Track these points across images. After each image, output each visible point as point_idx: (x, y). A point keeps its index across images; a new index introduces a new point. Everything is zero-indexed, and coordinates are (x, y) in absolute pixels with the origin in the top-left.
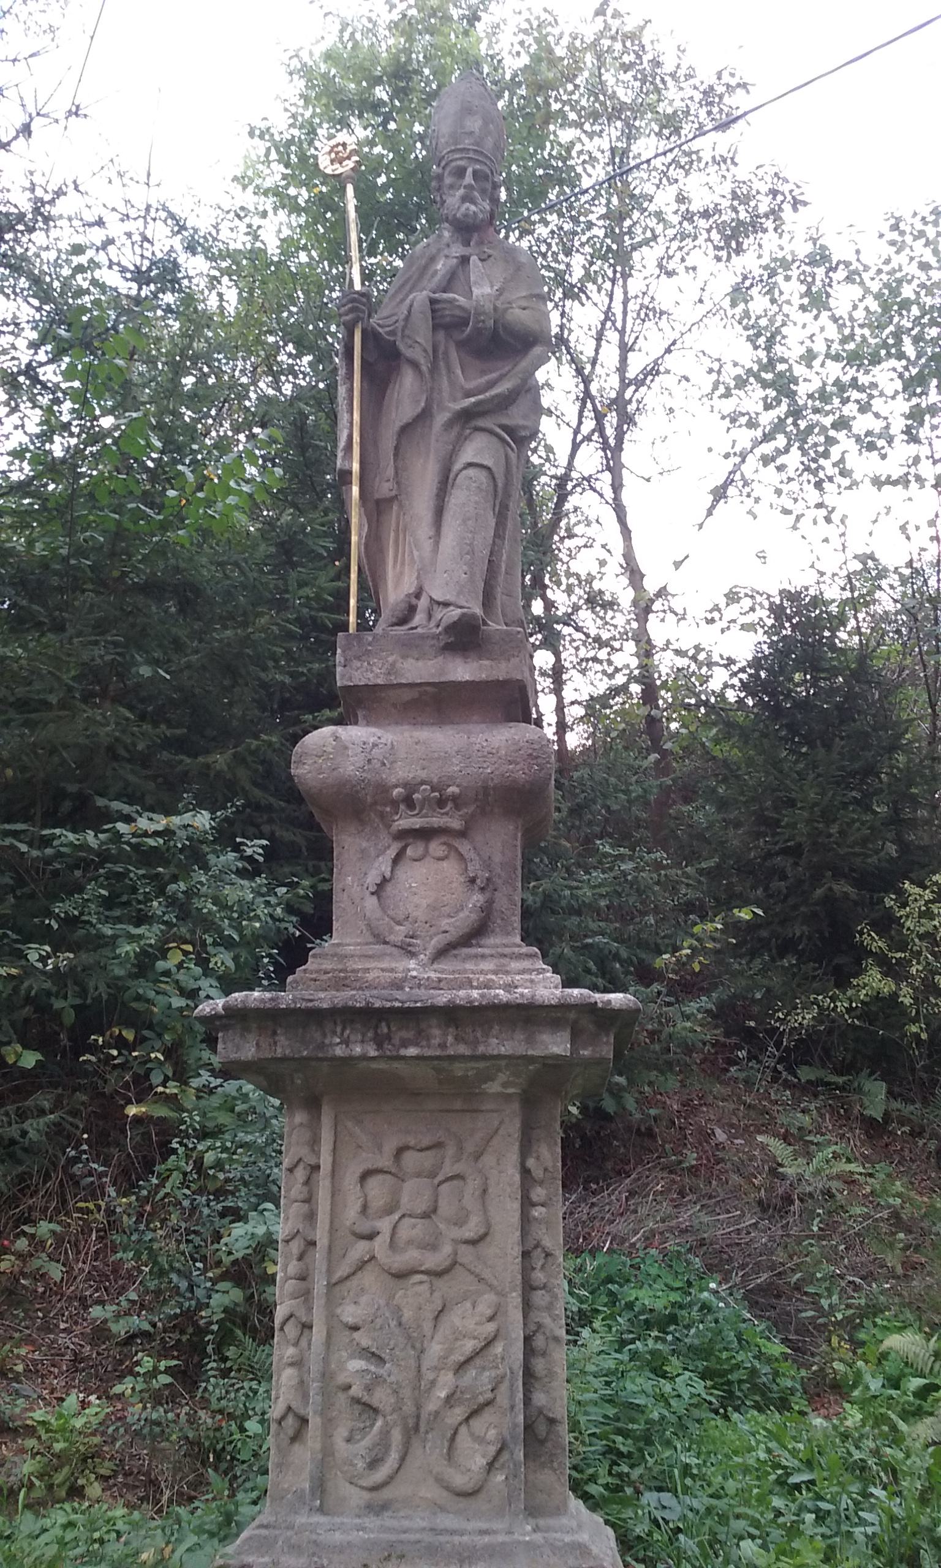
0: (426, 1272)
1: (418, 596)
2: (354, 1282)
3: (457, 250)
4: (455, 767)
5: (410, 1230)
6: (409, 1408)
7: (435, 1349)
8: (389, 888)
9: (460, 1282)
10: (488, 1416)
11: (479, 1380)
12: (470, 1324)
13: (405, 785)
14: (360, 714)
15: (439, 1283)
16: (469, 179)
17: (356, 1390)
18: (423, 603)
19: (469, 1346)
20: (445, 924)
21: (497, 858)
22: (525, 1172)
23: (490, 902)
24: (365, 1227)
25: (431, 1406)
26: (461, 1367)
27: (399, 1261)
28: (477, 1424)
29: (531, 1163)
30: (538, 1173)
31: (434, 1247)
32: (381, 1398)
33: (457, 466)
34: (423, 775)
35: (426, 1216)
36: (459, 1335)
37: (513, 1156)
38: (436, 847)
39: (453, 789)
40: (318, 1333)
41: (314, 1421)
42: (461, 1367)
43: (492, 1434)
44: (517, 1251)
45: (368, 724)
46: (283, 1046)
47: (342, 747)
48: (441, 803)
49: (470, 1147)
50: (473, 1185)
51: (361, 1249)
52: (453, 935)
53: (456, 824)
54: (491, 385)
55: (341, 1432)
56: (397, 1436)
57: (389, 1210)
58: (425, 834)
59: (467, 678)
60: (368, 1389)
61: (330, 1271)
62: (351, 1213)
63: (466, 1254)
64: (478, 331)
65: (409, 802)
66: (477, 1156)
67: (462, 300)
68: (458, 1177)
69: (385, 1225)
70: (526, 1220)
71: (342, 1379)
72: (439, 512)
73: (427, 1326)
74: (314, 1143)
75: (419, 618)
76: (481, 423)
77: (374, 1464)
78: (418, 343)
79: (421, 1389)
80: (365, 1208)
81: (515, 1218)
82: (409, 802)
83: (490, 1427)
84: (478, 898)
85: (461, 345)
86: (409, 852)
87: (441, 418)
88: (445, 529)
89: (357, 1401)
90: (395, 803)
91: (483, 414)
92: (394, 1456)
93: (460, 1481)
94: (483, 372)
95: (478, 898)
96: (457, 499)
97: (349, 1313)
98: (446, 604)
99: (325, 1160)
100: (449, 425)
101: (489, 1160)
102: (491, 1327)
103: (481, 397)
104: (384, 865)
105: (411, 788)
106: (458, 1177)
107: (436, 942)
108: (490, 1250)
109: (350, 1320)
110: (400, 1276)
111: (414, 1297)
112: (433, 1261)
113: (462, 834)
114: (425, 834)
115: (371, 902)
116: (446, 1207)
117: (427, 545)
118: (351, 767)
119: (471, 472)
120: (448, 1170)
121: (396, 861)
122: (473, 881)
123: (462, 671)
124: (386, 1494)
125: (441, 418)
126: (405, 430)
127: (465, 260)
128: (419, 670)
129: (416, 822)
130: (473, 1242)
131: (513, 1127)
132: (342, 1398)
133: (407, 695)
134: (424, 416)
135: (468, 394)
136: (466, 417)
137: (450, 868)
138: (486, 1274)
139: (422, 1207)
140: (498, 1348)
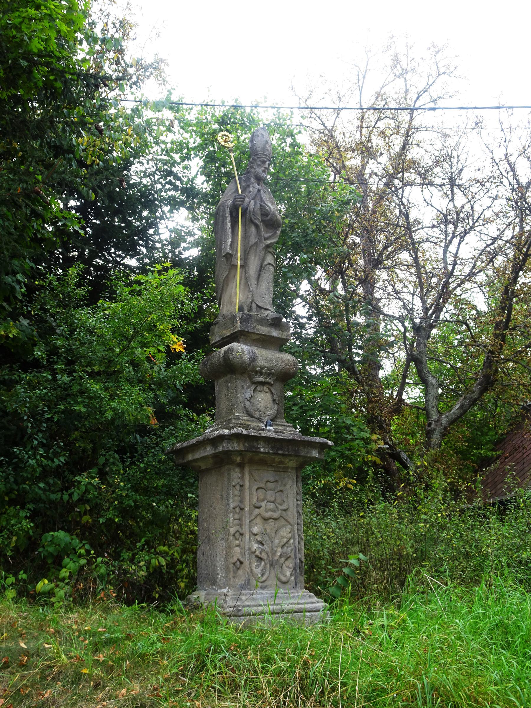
2: (254, 521)
5: (271, 506)
6: (271, 558)
7: (277, 541)
9: (282, 522)
10: (289, 561)
11: (288, 550)
12: (285, 534)
14: (241, 340)
15: (277, 522)
17: (257, 553)
18: (254, 305)
19: (285, 540)
24: (258, 505)
25: (276, 558)
26: (283, 547)
27: (269, 514)
28: (286, 562)
32: (264, 556)
33: (265, 263)
35: (273, 502)
36: (283, 537)
38: (266, 388)
39: (273, 371)
40: (247, 536)
41: (247, 563)
42: (283, 547)
43: (291, 565)
47: (243, 351)
50: (285, 493)
51: (257, 511)
56: (268, 566)
57: (263, 500)
58: (263, 384)
59: (276, 335)
60: (261, 553)
61: (249, 517)
62: (255, 500)
64: (271, 220)
68: (282, 491)
69: (263, 504)
71: (253, 550)
73: (273, 535)
74: (242, 478)
76: (269, 250)
77: (263, 575)
79: (274, 553)
80: (257, 500)
82: (261, 374)
83: (290, 563)
86: (258, 388)
89: (257, 556)
90: (256, 372)
92: (267, 572)
93: (284, 579)
96: (264, 274)
99: (247, 483)
100: (263, 248)
102: (290, 535)
105: (262, 368)
106: (282, 491)
108: (289, 513)
109: (255, 532)
111: (271, 526)
112: (275, 515)
114: (263, 384)
115: (248, 403)
116: (279, 500)
120: (279, 488)
121: (254, 391)
124: (265, 584)
127: (259, 190)
129: (262, 379)
130: (285, 510)
132: (253, 556)
133: (258, 337)
135: (266, 239)
137: (269, 395)
138: (289, 520)
139: (273, 500)
140: (292, 541)
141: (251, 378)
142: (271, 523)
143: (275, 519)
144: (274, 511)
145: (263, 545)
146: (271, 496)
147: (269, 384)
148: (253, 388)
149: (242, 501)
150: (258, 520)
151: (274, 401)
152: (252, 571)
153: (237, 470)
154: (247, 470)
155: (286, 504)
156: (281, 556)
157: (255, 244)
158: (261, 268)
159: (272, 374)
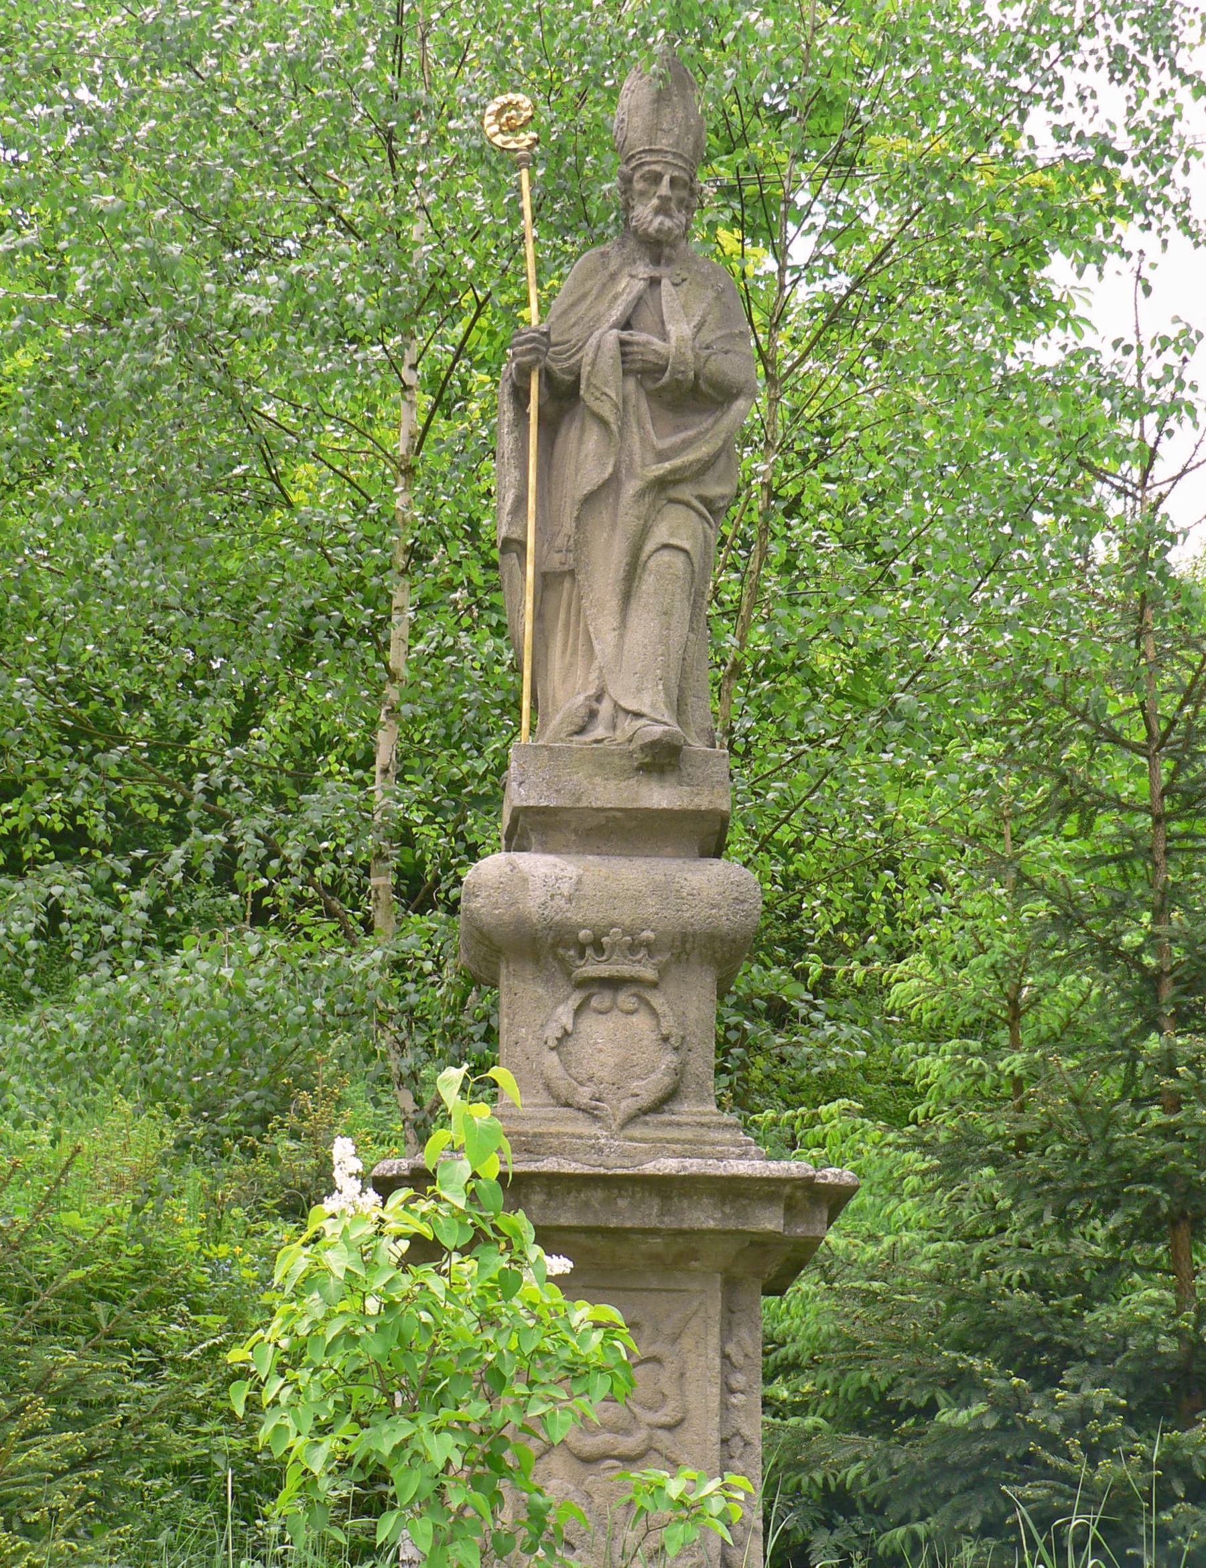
0: (619, 1458)
1: (599, 698)
3: (644, 270)
4: (651, 907)
8: (571, 1045)
13: (592, 928)
16: (664, 189)
18: (605, 708)
20: (635, 1085)
21: (693, 1014)
22: (725, 1357)
23: (684, 1064)
27: (590, 1445)
29: (731, 1349)
30: (738, 1359)
31: (627, 1432)
33: (649, 547)
34: (615, 916)
37: (714, 1340)
38: (626, 999)
39: (648, 934)
44: (715, 1437)
45: (545, 849)
48: (633, 948)
49: (667, 1329)
50: (671, 1367)
52: (646, 1100)
53: (649, 973)
54: (686, 445)
58: (614, 984)
59: (664, 805)
65: (599, 948)
66: (675, 1339)
67: (658, 344)
70: (725, 1407)
75: (599, 731)
76: (673, 493)
78: (605, 387)
81: (715, 1404)
82: (599, 948)
84: (669, 1059)
85: (654, 396)
86: (594, 1003)
87: (631, 488)
88: (633, 622)
90: (581, 949)
91: (676, 483)
94: (677, 429)
95: (669, 1059)
96: (648, 583)
98: (638, 715)
100: (641, 494)
101: (687, 1342)
103: (677, 462)
104: (564, 1015)
107: (628, 1105)
108: (687, 1435)
110: (589, 1461)
112: (628, 1444)
113: (654, 985)
114: (614, 984)
117: (611, 637)
118: (533, 905)
119: (665, 556)
121: (578, 1012)
122: (666, 1039)
123: (659, 796)
125: (631, 488)
126: (590, 499)
127: (654, 282)
128: (608, 793)
130: (669, 1428)
131: (715, 1308)
134: (611, 485)
135: (662, 456)
136: (661, 484)
137: (642, 1022)
141: (566, 969)
148: (576, 999)
151: (666, 1039)
155: (671, 1404)
157: (606, 484)
159: (648, 945)
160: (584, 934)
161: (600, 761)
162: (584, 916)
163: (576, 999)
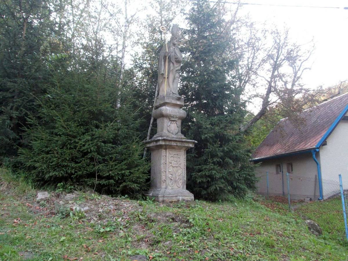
5: (176, 163)
7: (177, 174)
19: (180, 174)
26: (179, 176)
32: (172, 179)
38: (175, 122)
42: (179, 176)
46: (167, 143)
47: (167, 110)
55: (169, 182)
58: (174, 121)
63: (180, 165)
65: (173, 117)
69: (173, 162)
72: (173, 82)
73: (176, 172)
74: (166, 154)
79: (176, 178)
82: (173, 117)
83: (181, 181)
89: (170, 179)
90: (171, 117)
93: (179, 186)
97: (170, 171)
98: (175, 94)
99: (167, 155)
111: (175, 169)
112: (177, 166)
114: (174, 121)
116: (178, 161)
123: (178, 103)
125: (175, 70)
127: (174, 49)
128: (174, 102)
135: (176, 67)
137: (176, 125)
140: (182, 174)
141: (169, 119)
142: (175, 168)
143: (177, 167)
144: (176, 164)
145: (172, 175)
146: (175, 159)
147: (176, 121)
149: (166, 161)
150: (171, 167)
152: (168, 184)
153: (164, 151)
154: (167, 151)
156: (178, 179)
158: (174, 79)
160: (172, 116)
161: (173, 98)
162: (172, 114)
163: (170, 122)
